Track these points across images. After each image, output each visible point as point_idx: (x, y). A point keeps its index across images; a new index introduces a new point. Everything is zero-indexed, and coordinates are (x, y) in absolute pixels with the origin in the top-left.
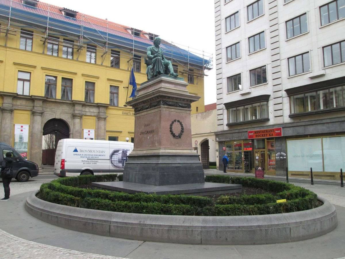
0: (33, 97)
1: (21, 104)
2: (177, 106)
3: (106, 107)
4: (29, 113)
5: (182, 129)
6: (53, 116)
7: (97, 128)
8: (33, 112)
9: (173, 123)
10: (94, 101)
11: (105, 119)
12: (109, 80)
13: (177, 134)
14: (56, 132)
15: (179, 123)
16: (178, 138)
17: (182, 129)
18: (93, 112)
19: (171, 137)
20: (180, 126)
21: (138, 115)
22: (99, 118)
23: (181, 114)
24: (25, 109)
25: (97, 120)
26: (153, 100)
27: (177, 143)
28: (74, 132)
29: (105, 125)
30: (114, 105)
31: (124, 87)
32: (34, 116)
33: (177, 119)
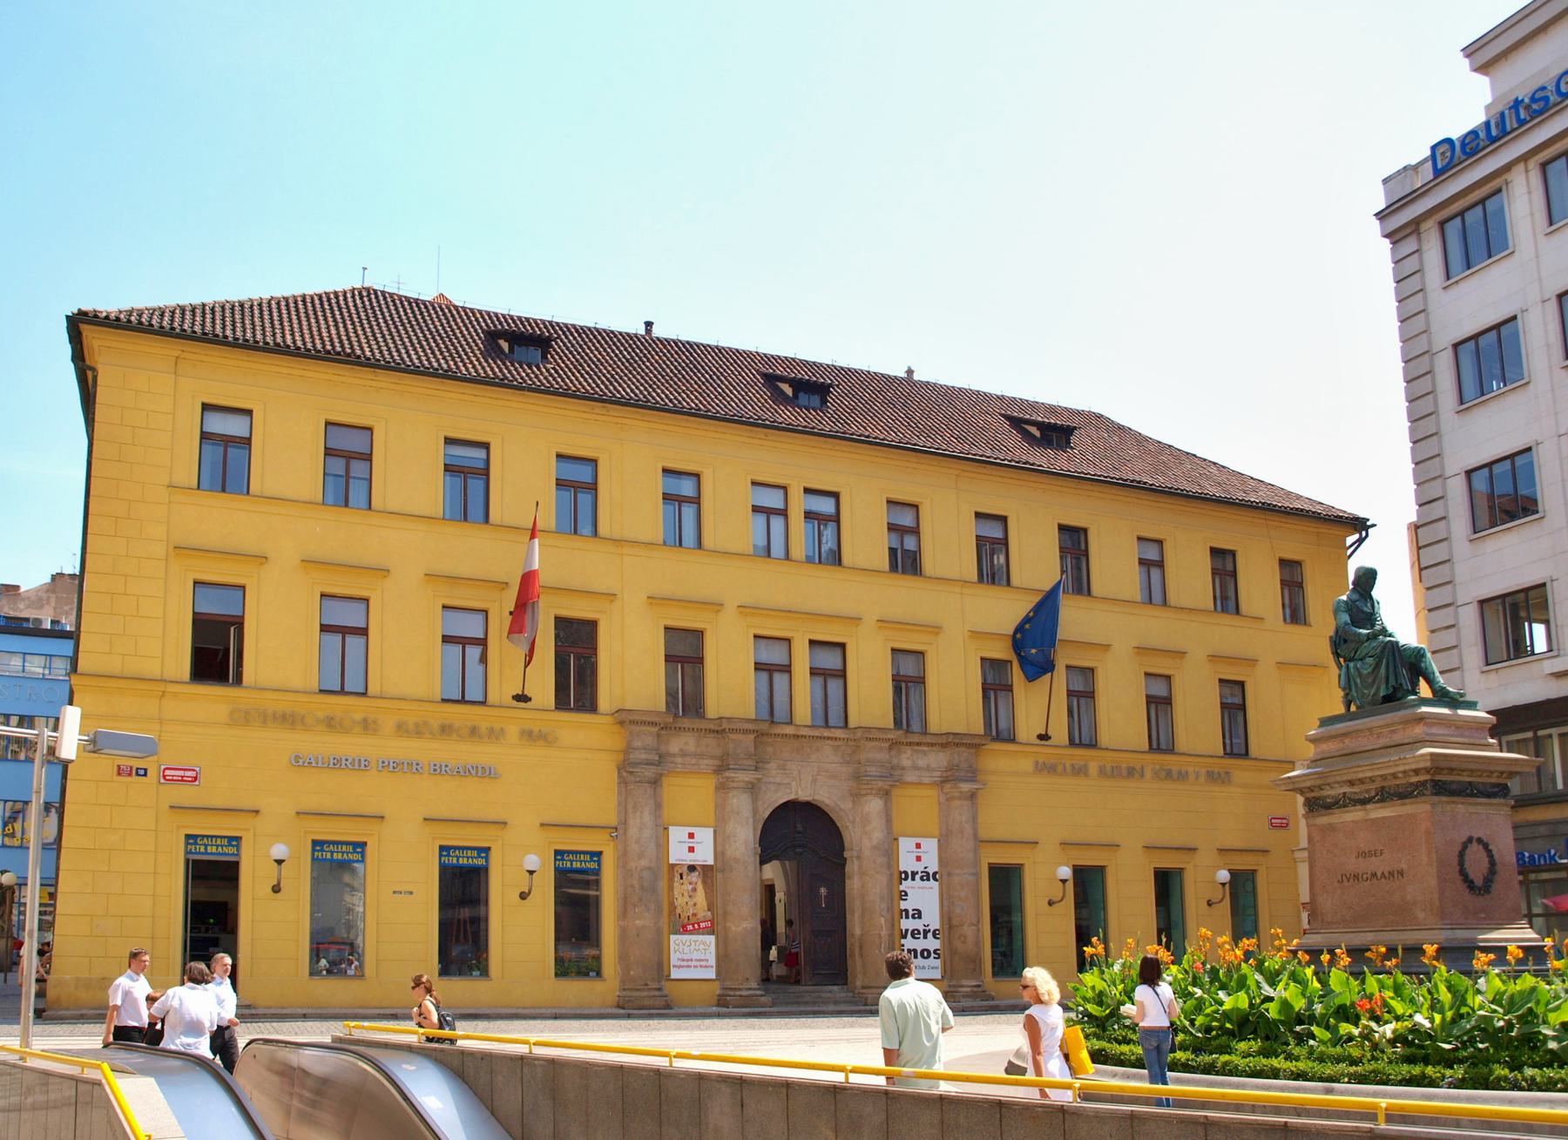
5: (1492, 863)
6: (788, 791)
13: (1479, 882)
14: (798, 850)
15: (1481, 847)
17: (1492, 863)
19: (1461, 886)
20: (1485, 854)
33: (1476, 836)
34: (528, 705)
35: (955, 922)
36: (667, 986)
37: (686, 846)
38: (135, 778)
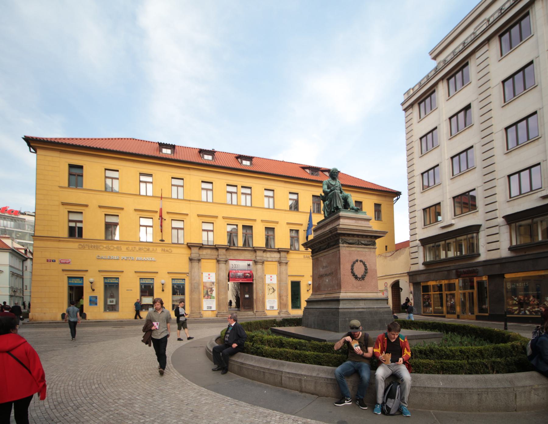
0: (217, 246)
1: (206, 253)
2: (358, 244)
3: (287, 251)
4: (215, 261)
5: (366, 269)
7: (279, 273)
8: (218, 260)
9: (354, 263)
10: (274, 246)
11: (287, 263)
12: (288, 223)
15: (362, 263)
16: (361, 279)
17: (366, 269)
18: (274, 258)
19: (353, 278)
20: (363, 266)
21: (315, 257)
22: (280, 263)
23: (364, 252)
24: (210, 258)
25: (278, 265)
26: (331, 239)
27: (361, 286)
28: (257, 278)
29: (287, 270)
30: (295, 250)
31: (304, 230)
32: (218, 264)
33: (359, 259)
34: (164, 242)
35: (281, 295)
36: (202, 312)
37: (208, 278)
38: (52, 263)
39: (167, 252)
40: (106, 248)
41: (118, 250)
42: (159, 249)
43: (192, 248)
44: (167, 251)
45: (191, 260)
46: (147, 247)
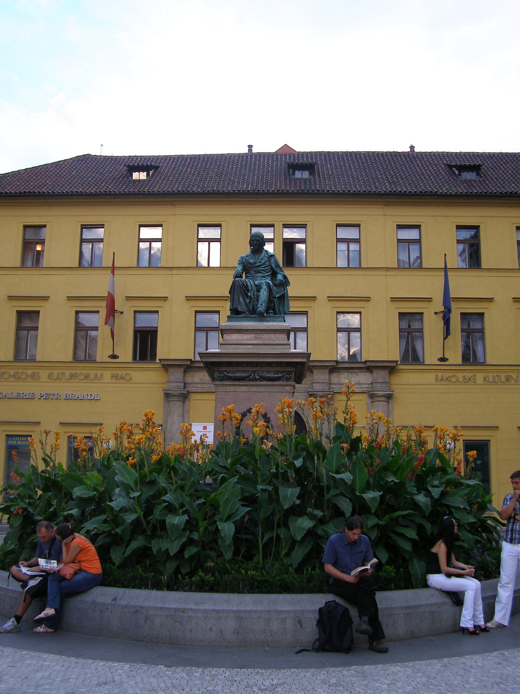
1: (201, 380)
25: (369, 401)
39: (122, 381)
40: (14, 376)
41: (34, 379)
42: (107, 374)
43: (171, 370)
44: (122, 378)
45: (167, 395)
46: (84, 372)
